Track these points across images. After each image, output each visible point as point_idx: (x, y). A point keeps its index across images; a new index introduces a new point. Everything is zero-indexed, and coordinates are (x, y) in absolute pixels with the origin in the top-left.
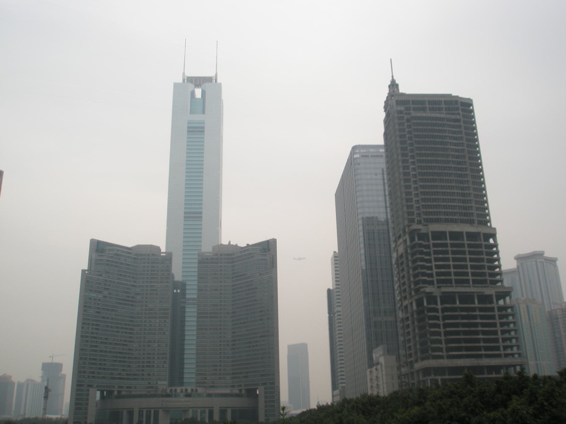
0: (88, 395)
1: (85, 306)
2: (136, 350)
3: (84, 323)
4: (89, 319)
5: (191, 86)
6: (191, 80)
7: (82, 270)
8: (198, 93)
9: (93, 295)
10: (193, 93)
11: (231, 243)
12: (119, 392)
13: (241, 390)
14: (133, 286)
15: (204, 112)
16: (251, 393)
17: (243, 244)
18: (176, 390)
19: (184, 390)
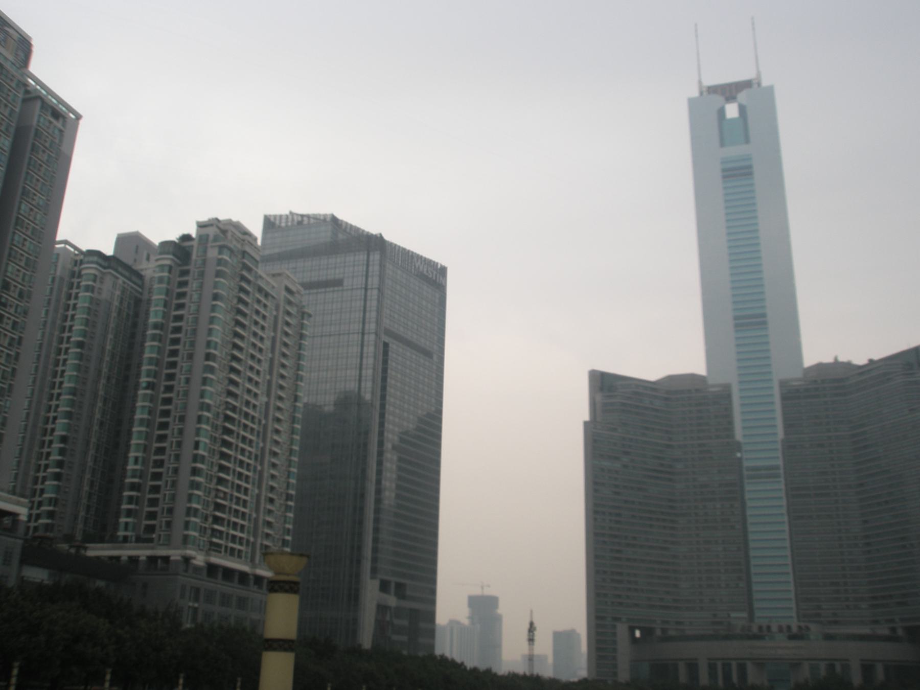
0: (614, 634)
1: (595, 483)
3: (596, 512)
5: (718, 99)
6: (713, 90)
8: (732, 111)
10: (721, 112)
12: (664, 631)
13: (893, 630)
17: (860, 360)
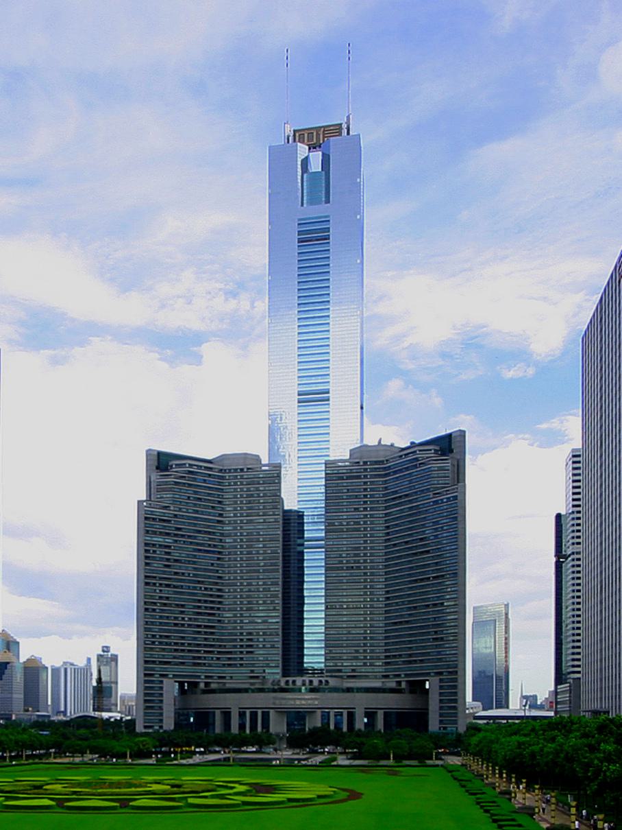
2: (229, 622)
4: (155, 577)
7: (139, 502)
9: (158, 539)
11: (383, 443)
13: (399, 683)
14: (219, 522)
15: (328, 201)
16: (417, 687)
18: (294, 682)
19: (307, 682)
